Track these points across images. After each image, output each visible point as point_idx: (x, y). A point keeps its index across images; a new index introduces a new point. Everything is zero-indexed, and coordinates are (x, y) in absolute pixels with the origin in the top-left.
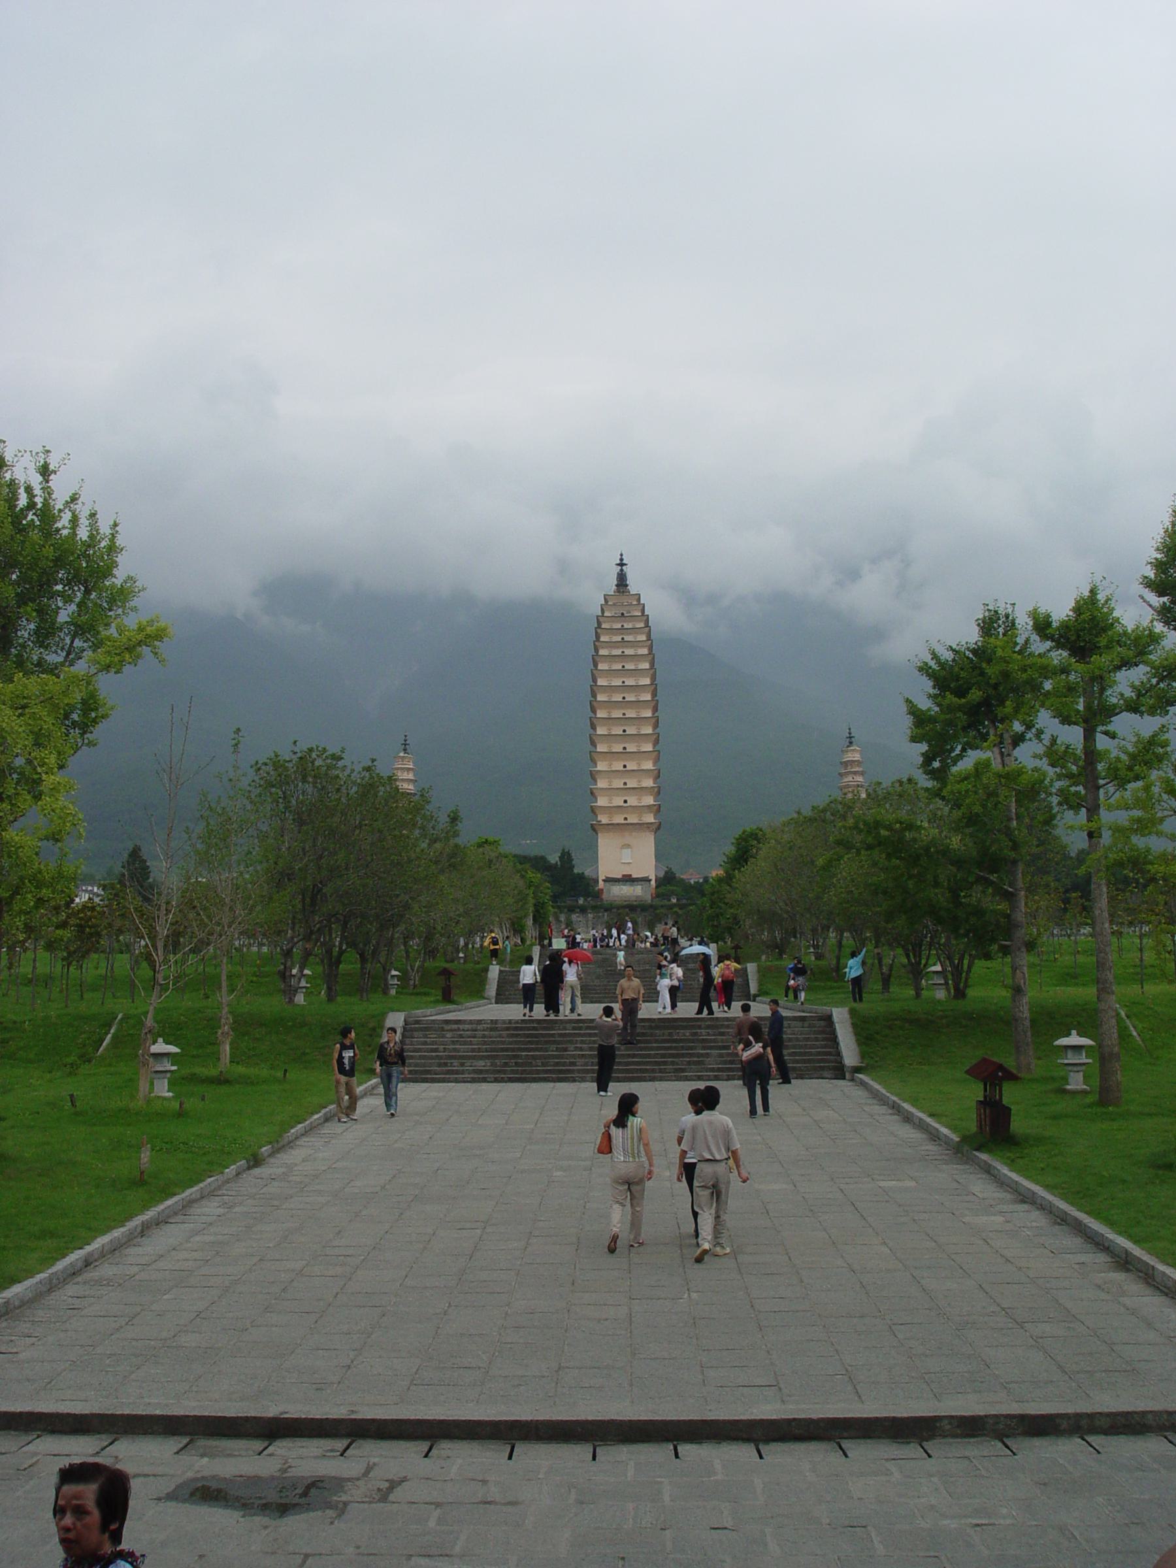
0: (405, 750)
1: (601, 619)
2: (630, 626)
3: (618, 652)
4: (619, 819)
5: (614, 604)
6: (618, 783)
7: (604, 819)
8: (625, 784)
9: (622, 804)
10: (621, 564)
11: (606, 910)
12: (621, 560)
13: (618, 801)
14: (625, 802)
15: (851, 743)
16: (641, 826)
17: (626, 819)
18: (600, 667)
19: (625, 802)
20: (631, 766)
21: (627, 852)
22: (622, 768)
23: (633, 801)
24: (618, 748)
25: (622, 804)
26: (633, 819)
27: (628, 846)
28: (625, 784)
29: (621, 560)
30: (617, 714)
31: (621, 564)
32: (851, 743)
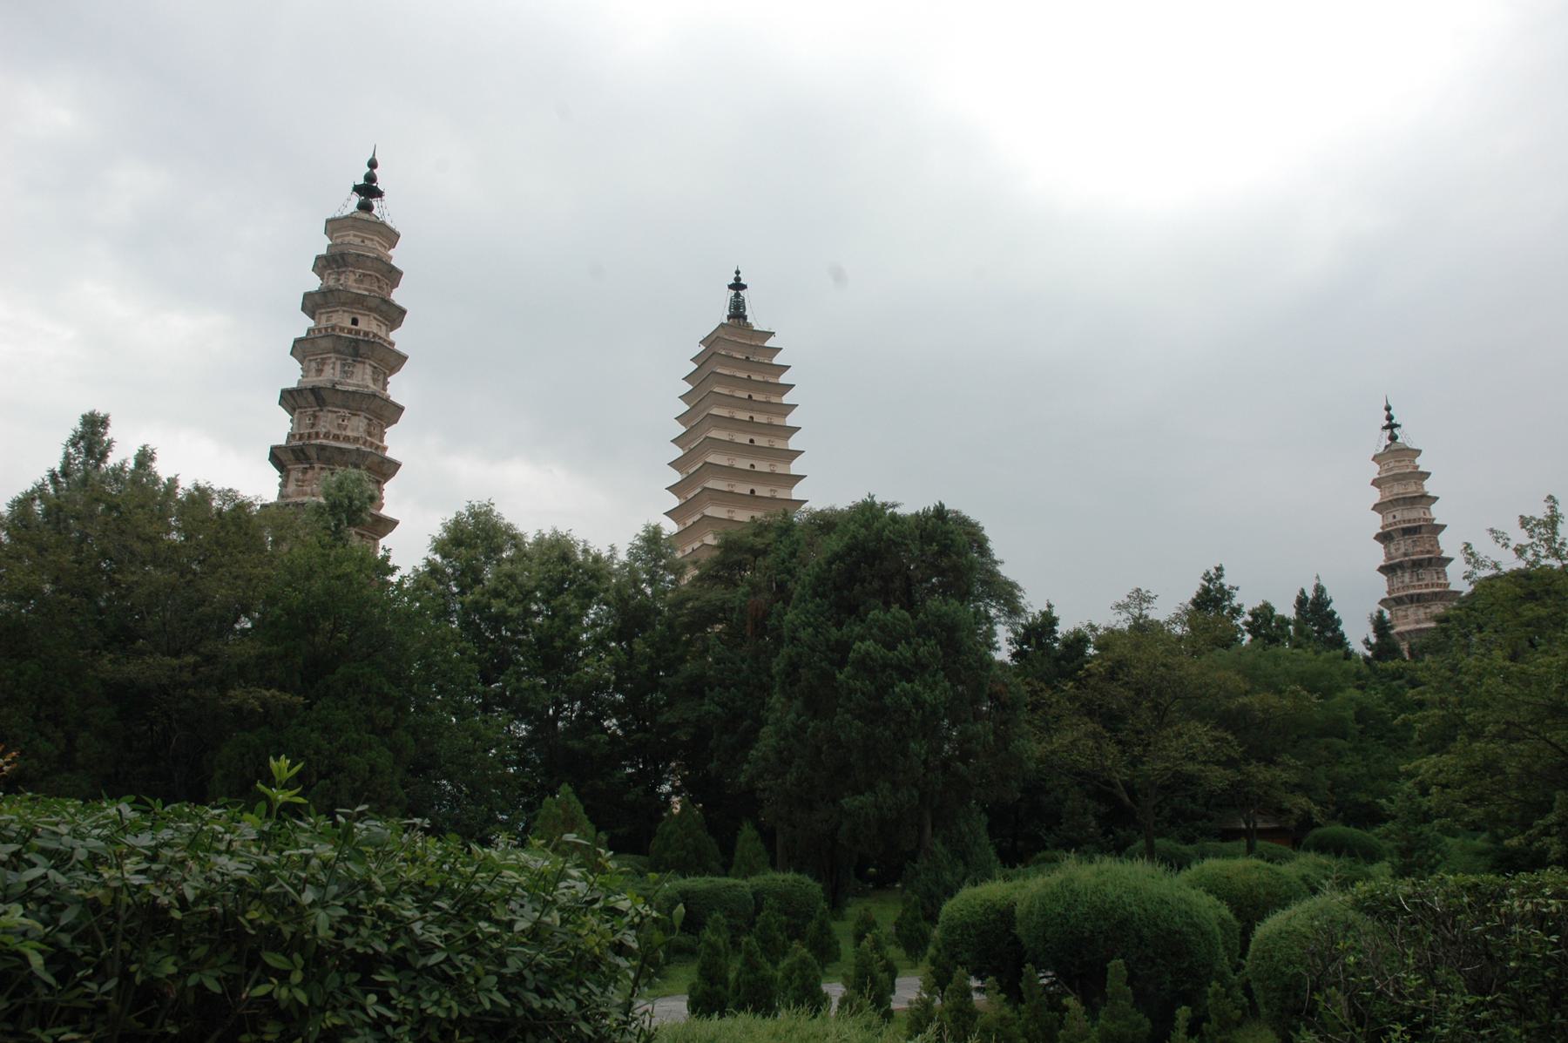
10: (738, 286)
12: (738, 279)
15: (1393, 438)
29: (738, 279)
31: (738, 286)
32: (1393, 438)
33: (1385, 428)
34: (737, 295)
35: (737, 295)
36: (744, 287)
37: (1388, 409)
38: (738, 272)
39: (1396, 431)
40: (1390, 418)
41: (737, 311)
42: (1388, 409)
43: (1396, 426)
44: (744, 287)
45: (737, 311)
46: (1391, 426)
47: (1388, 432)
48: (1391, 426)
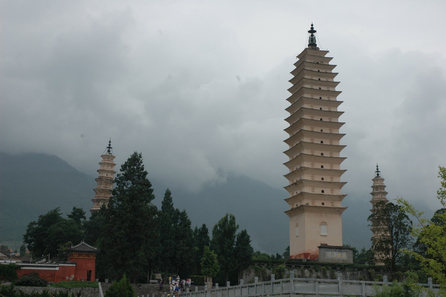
0: (109, 151)
2: (324, 71)
3: (317, 87)
4: (318, 204)
5: (311, 55)
10: (312, 31)
11: (359, 270)
12: (312, 28)
13: (318, 191)
15: (378, 175)
17: (323, 204)
19: (323, 191)
20: (327, 167)
21: (324, 227)
22: (320, 168)
23: (327, 192)
24: (318, 153)
27: (324, 223)
28: (323, 179)
29: (312, 28)
30: (317, 129)
31: (312, 31)
32: (378, 175)
34: (312, 35)
35: (312, 35)
37: (377, 167)
38: (312, 25)
40: (377, 169)
41: (312, 43)
42: (377, 167)
45: (312, 43)
46: (378, 172)
47: (377, 173)
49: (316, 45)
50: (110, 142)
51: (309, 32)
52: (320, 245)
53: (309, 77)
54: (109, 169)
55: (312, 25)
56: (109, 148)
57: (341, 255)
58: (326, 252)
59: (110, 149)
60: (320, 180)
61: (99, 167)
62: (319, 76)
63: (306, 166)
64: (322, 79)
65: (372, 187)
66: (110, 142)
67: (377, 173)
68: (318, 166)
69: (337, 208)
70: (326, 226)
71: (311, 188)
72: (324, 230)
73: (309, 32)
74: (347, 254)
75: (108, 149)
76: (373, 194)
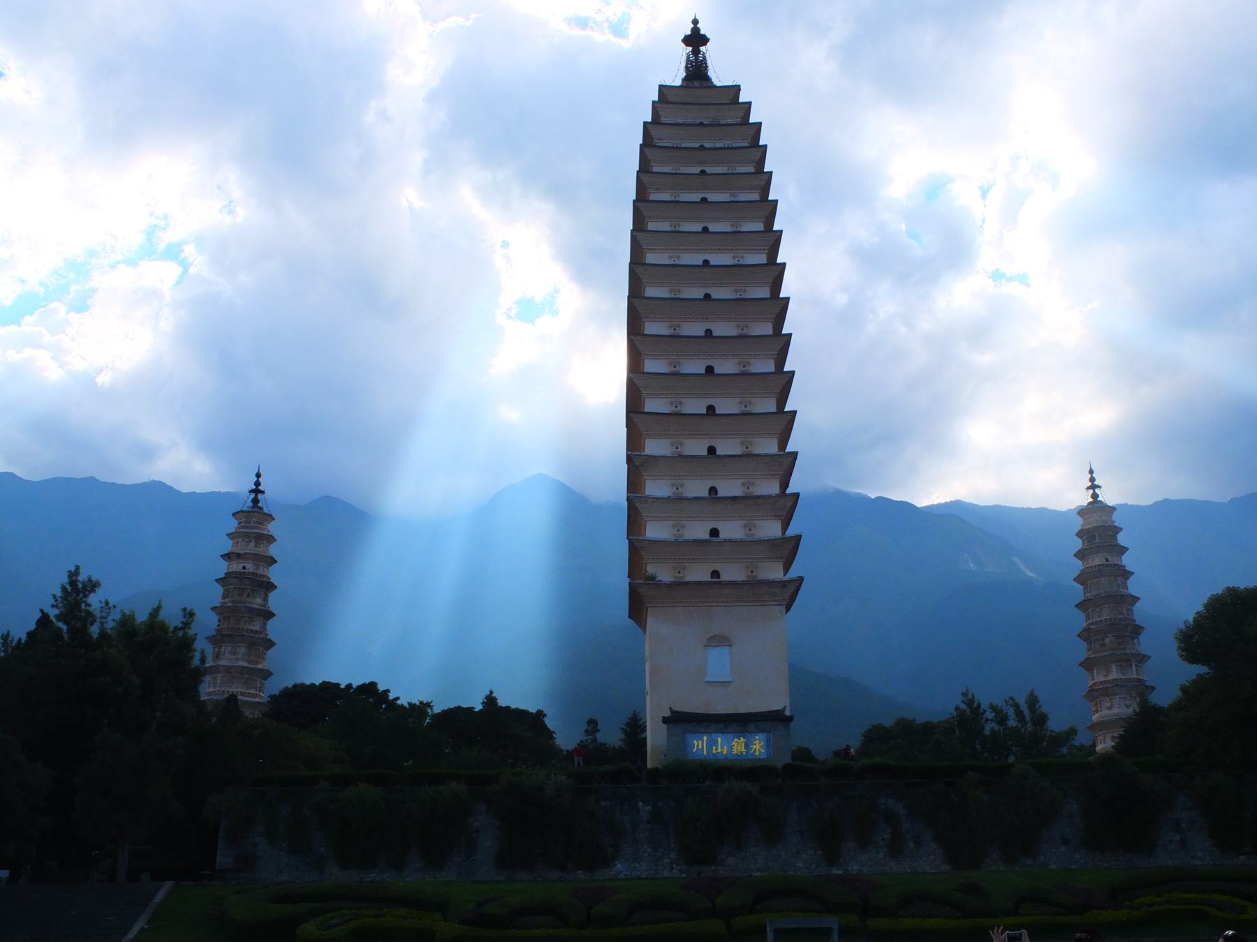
1: (651, 128)
3: (696, 197)
4: (698, 573)
6: (697, 488)
7: (665, 575)
8: (713, 490)
9: (706, 536)
12: (696, 30)
13: (698, 531)
14: (714, 533)
16: (755, 591)
17: (715, 574)
18: (651, 226)
19: (714, 533)
23: (731, 530)
25: (705, 535)
26: (732, 572)
27: (720, 640)
28: (713, 490)
29: (696, 30)
31: (696, 39)
32: (1095, 496)
33: (1088, 488)
34: (696, 52)
35: (696, 52)
36: (704, 40)
38: (695, 22)
39: (1097, 491)
41: (697, 71)
43: (1099, 487)
44: (704, 40)
45: (697, 71)
46: (1093, 487)
47: (1091, 492)
48: (1093, 487)
49: (708, 79)
50: (258, 475)
51: (687, 41)
52: (668, 714)
53: (667, 169)
54: (251, 548)
55: (695, 22)
56: (257, 491)
57: (747, 746)
58: (688, 736)
59: (260, 496)
60: (705, 494)
61: (228, 546)
62: (701, 163)
63: (657, 454)
64: (709, 170)
65: (1080, 534)
66: (258, 475)
67: (1091, 492)
68: (697, 447)
69: (761, 582)
70: (726, 650)
71: (671, 523)
72: (718, 663)
73: (687, 41)
74: (768, 740)
75: (253, 495)
76: (1080, 555)
